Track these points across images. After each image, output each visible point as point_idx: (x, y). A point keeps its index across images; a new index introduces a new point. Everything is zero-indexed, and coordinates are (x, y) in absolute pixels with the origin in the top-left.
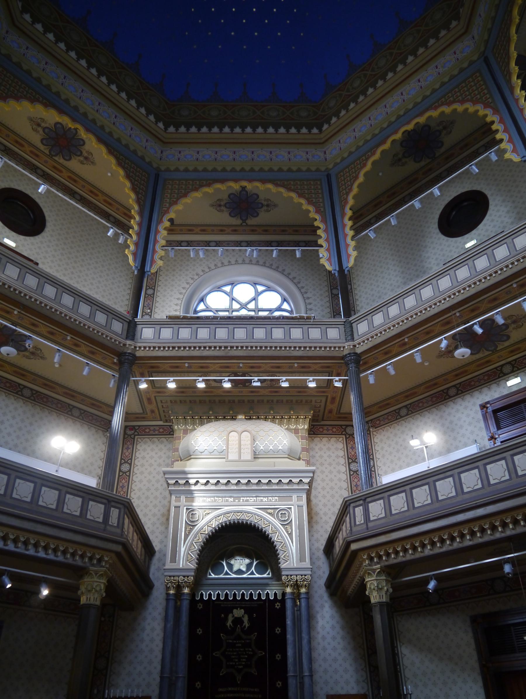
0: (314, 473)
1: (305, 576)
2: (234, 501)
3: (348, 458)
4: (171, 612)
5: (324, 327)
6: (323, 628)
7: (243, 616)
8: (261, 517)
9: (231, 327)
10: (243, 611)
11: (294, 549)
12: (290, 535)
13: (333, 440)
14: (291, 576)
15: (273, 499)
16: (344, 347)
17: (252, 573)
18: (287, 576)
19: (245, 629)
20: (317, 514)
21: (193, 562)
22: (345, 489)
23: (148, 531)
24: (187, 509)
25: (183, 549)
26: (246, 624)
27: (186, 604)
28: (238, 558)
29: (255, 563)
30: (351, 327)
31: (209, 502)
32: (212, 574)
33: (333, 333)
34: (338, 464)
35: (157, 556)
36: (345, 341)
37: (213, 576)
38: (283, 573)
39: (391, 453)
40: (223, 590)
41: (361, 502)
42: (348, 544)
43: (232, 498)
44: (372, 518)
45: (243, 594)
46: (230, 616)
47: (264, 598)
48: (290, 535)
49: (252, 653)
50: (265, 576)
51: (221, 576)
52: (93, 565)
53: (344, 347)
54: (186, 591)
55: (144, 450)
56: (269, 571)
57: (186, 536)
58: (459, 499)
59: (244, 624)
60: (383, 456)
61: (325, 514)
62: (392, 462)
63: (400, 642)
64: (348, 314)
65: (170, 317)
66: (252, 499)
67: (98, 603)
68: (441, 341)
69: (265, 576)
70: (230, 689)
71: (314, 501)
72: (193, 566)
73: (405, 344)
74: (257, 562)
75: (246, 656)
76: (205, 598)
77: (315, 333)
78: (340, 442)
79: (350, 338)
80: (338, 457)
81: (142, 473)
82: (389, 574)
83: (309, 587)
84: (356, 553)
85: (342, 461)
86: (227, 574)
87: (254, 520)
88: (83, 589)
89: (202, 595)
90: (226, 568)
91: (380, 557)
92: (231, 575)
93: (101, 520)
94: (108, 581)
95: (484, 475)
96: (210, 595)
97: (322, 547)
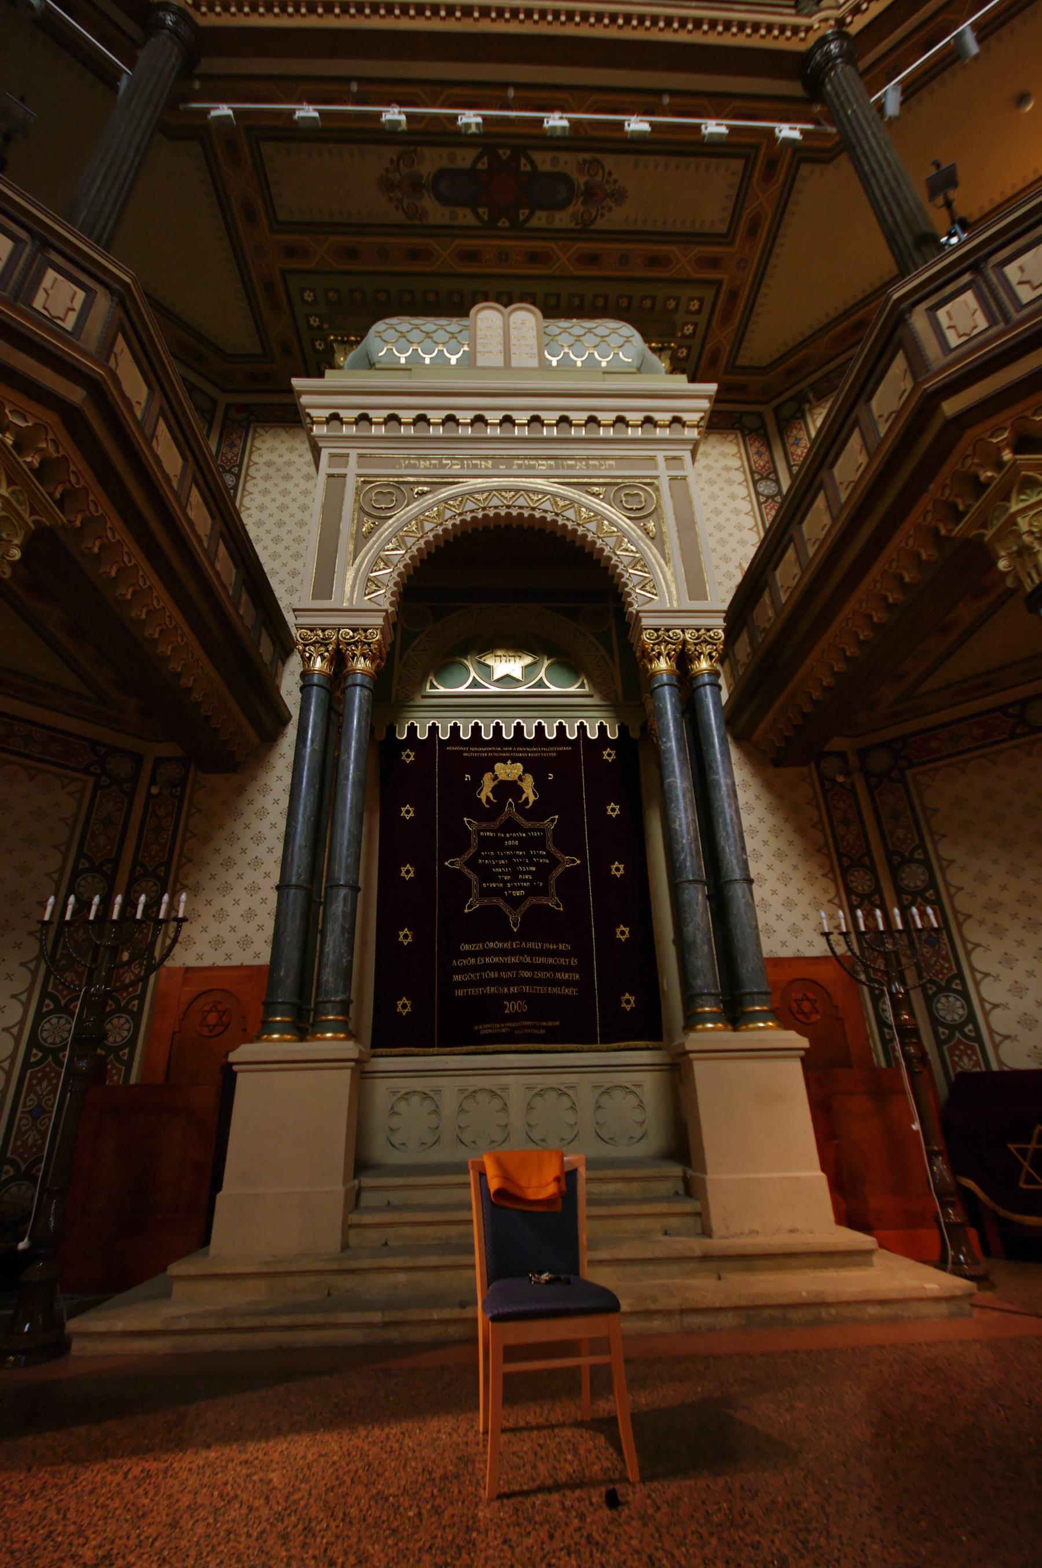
1: (708, 630)
2: (494, 467)
3: (752, 472)
7: (520, 778)
8: (573, 502)
10: (519, 767)
14: (667, 630)
15: (601, 465)
18: (657, 630)
19: (528, 807)
22: (751, 529)
26: (529, 794)
31: (426, 468)
32: (439, 686)
34: (730, 482)
38: (645, 622)
41: (967, 278)
43: (490, 462)
46: (487, 777)
49: (547, 861)
51: (462, 689)
55: (272, 450)
59: (524, 797)
63: (931, 832)
66: (543, 465)
70: (491, 945)
74: (549, 662)
75: (534, 869)
76: (422, 735)
78: (731, 441)
85: (739, 477)
89: (412, 729)
92: (487, 688)
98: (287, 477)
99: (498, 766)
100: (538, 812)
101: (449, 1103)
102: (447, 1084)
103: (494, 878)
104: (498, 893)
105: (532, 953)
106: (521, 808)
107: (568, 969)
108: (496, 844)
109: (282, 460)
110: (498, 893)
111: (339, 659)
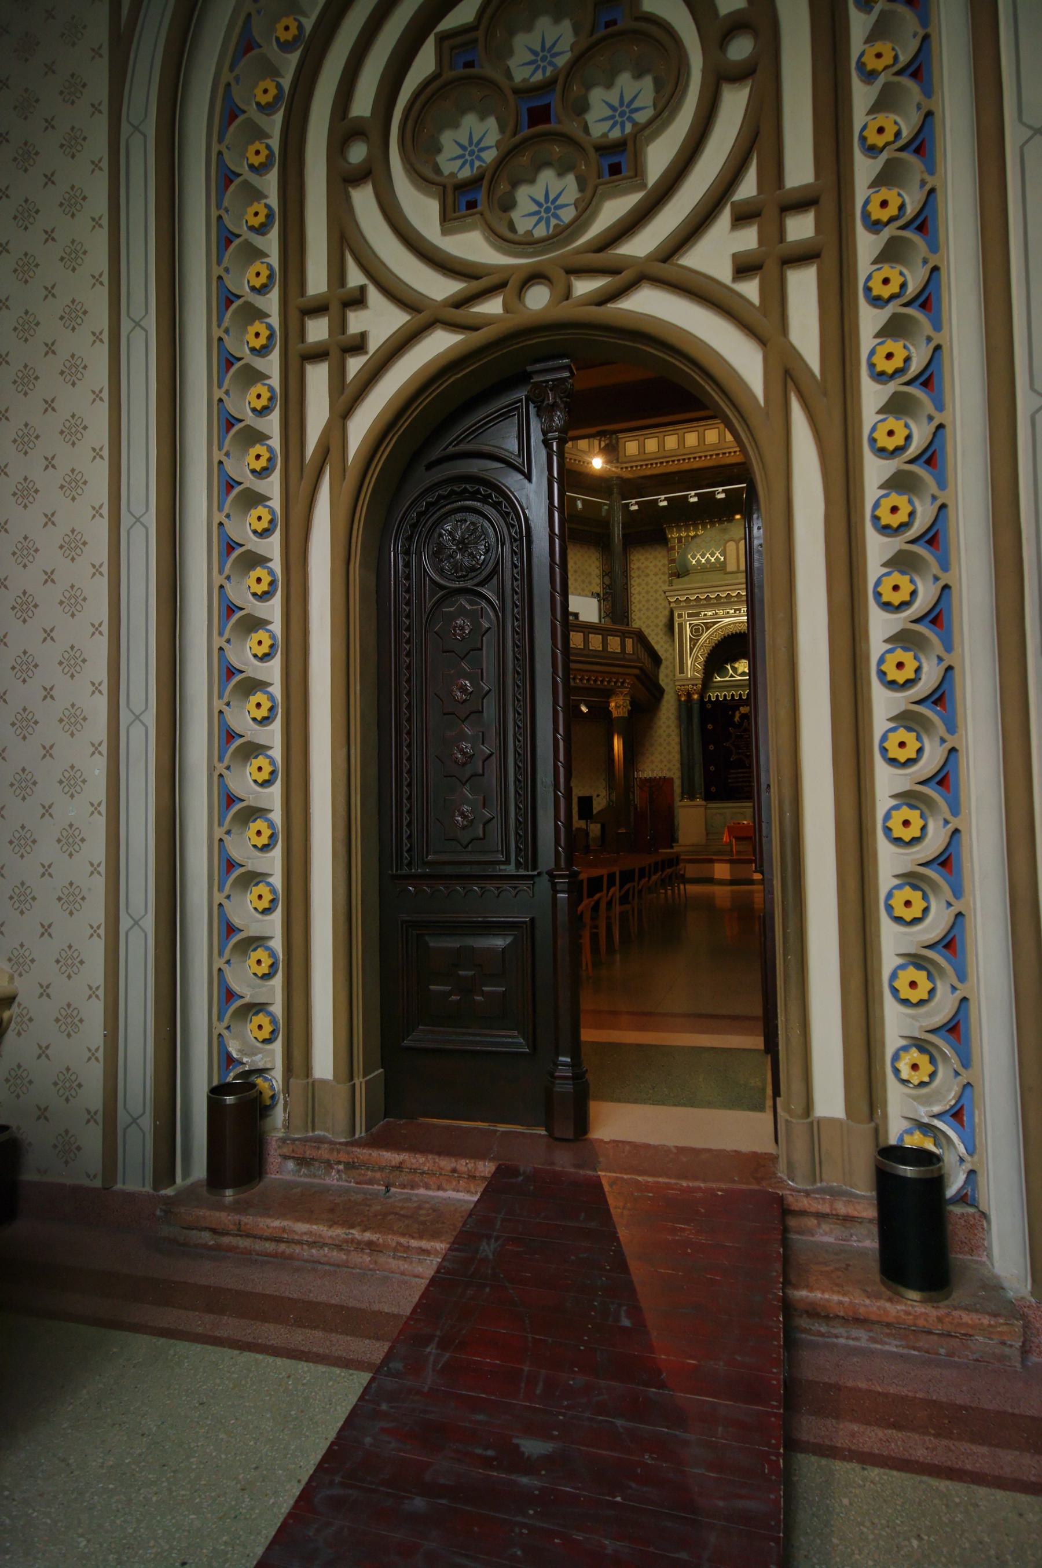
21: (701, 672)
23: (653, 643)
24: (690, 624)
25: (689, 662)
27: (696, 708)
35: (664, 664)
37: (719, 679)
40: (729, 692)
46: (737, 713)
52: (619, 687)
55: (639, 560)
57: (691, 650)
67: (626, 715)
81: (639, 585)
86: (732, 676)
88: (613, 704)
89: (710, 696)
90: (731, 672)
93: (619, 651)
94: (631, 698)
96: (717, 696)
98: (647, 575)
109: (643, 566)
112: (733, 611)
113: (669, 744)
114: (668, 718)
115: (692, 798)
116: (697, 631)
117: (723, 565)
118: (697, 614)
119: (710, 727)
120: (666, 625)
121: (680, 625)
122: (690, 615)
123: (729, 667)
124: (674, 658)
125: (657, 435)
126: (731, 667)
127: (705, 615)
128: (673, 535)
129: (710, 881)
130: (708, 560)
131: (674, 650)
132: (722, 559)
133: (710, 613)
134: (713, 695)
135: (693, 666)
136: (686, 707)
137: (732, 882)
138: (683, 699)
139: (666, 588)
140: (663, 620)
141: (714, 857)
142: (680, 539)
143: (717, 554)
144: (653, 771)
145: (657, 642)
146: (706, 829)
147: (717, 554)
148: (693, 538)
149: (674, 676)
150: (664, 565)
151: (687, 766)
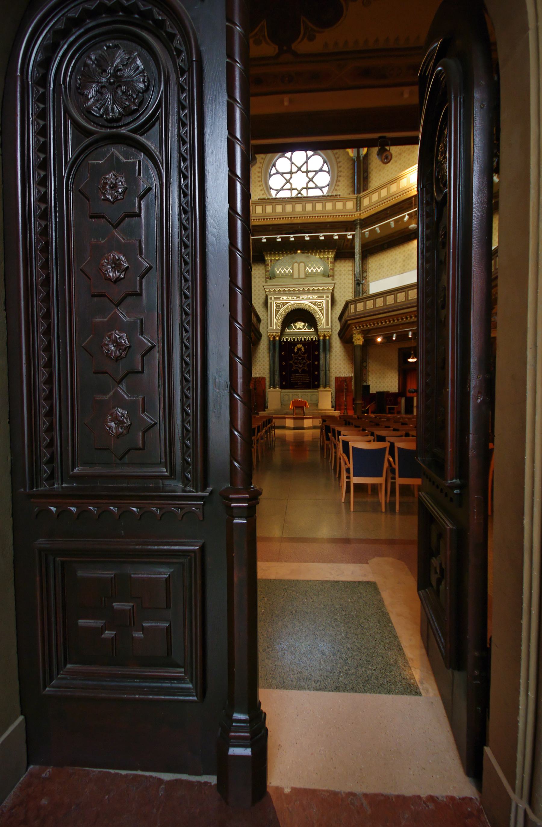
0: (335, 284)
4: (271, 347)
5: (344, 201)
6: (336, 352)
9: (294, 203)
10: (301, 345)
11: (324, 320)
12: (323, 314)
13: (347, 261)
16: (354, 215)
17: (305, 329)
20: (336, 301)
23: (257, 311)
24: (276, 303)
25: (275, 321)
27: (277, 344)
28: (299, 323)
29: (307, 325)
30: (360, 200)
33: (350, 205)
34: (349, 274)
35: (262, 322)
36: (355, 210)
37: (288, 331)
38: (319, 331)
39: (376, 270)
42: (347, 321)
44: (358, 310)
45: (301, 339)
47: (310, 340)
48: (323, 314)
50: (311, 330)
51: (292, 331)
53: (354, 215)
54: (277, 338)
56: (313, 328)
58: (395, 305)
60: (372, 271)
61: (340, 301)
62: (376, 274)
64: (359, 192)
65: (260, 199)
68: (404, 216)
69: (311, 330)
71: (336, 295)
72: (279, 328)
73: (387, 214)
77: (339, 205)
79: (358, 208)
80: (349, 270)
82: (363, 333)
83: (330, 337)
84: (350, 325)
87: (307, 308)
89: (283, 339)
90: (293, 327)
91: (360, 327)
95: (407, 295)
96: (287, 339)
97: (338, 317)
99: (298, 345)
100: (304, 353)
101: (291, 396)
102: (291, 394)
103: (297, 364)
104: (297, 367)
105: (302, 376)
106: (301, 352)
107: (308, 378)
108: (297, 359)
110: (297, 367)
111: (274, 337)
112: (296, 298)
113: (264, 361)
114: (264, 349)
115: (274, 387)
116: (279, 306)
117: (292, 275)
118: (279, 298)
119: (283, 353)
120: (263, 303)
121: (271, 303)
122: (275, 298)
123: (293, 325)
124: (267, 320)
125: (262, 204)
126: (294, 325)
127: (283, 299)
128: (268, 258)
129: (284, 427)
130: (285, 272)
131: (267, 315)
132: (291, 271)
133: (285, 298)
134: (285, 338)
135: (276, 324)
136: (272, 343)
137: (295, 428)
138: (271, 339)
139: (264, 284)
140: (262, 300)
141: (286, 416)
142: (271, 261)
143: (289, 269)
144: (256, 374)
145: (259, 311)
146: (281, 402)
147: (289, 269)
148: (277, 260)
149: (267, 328)
150: (263, 273)
151: (272, 372)
